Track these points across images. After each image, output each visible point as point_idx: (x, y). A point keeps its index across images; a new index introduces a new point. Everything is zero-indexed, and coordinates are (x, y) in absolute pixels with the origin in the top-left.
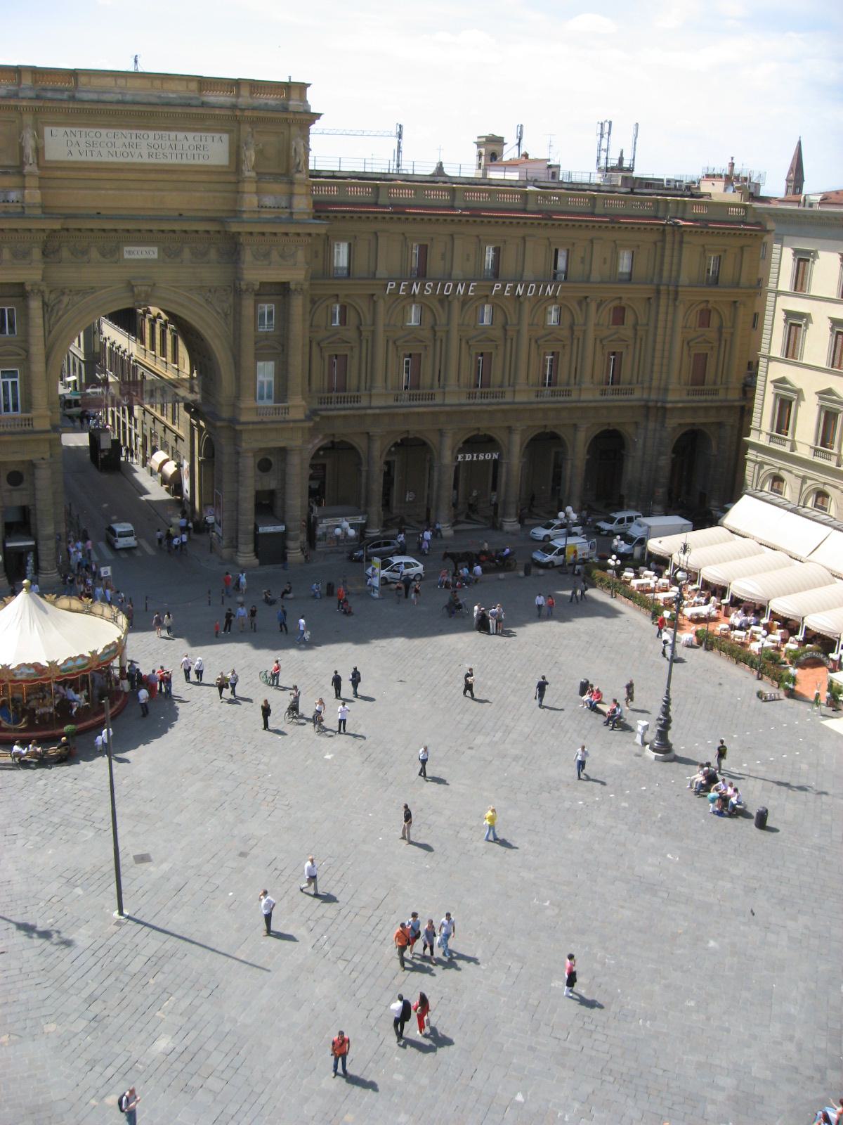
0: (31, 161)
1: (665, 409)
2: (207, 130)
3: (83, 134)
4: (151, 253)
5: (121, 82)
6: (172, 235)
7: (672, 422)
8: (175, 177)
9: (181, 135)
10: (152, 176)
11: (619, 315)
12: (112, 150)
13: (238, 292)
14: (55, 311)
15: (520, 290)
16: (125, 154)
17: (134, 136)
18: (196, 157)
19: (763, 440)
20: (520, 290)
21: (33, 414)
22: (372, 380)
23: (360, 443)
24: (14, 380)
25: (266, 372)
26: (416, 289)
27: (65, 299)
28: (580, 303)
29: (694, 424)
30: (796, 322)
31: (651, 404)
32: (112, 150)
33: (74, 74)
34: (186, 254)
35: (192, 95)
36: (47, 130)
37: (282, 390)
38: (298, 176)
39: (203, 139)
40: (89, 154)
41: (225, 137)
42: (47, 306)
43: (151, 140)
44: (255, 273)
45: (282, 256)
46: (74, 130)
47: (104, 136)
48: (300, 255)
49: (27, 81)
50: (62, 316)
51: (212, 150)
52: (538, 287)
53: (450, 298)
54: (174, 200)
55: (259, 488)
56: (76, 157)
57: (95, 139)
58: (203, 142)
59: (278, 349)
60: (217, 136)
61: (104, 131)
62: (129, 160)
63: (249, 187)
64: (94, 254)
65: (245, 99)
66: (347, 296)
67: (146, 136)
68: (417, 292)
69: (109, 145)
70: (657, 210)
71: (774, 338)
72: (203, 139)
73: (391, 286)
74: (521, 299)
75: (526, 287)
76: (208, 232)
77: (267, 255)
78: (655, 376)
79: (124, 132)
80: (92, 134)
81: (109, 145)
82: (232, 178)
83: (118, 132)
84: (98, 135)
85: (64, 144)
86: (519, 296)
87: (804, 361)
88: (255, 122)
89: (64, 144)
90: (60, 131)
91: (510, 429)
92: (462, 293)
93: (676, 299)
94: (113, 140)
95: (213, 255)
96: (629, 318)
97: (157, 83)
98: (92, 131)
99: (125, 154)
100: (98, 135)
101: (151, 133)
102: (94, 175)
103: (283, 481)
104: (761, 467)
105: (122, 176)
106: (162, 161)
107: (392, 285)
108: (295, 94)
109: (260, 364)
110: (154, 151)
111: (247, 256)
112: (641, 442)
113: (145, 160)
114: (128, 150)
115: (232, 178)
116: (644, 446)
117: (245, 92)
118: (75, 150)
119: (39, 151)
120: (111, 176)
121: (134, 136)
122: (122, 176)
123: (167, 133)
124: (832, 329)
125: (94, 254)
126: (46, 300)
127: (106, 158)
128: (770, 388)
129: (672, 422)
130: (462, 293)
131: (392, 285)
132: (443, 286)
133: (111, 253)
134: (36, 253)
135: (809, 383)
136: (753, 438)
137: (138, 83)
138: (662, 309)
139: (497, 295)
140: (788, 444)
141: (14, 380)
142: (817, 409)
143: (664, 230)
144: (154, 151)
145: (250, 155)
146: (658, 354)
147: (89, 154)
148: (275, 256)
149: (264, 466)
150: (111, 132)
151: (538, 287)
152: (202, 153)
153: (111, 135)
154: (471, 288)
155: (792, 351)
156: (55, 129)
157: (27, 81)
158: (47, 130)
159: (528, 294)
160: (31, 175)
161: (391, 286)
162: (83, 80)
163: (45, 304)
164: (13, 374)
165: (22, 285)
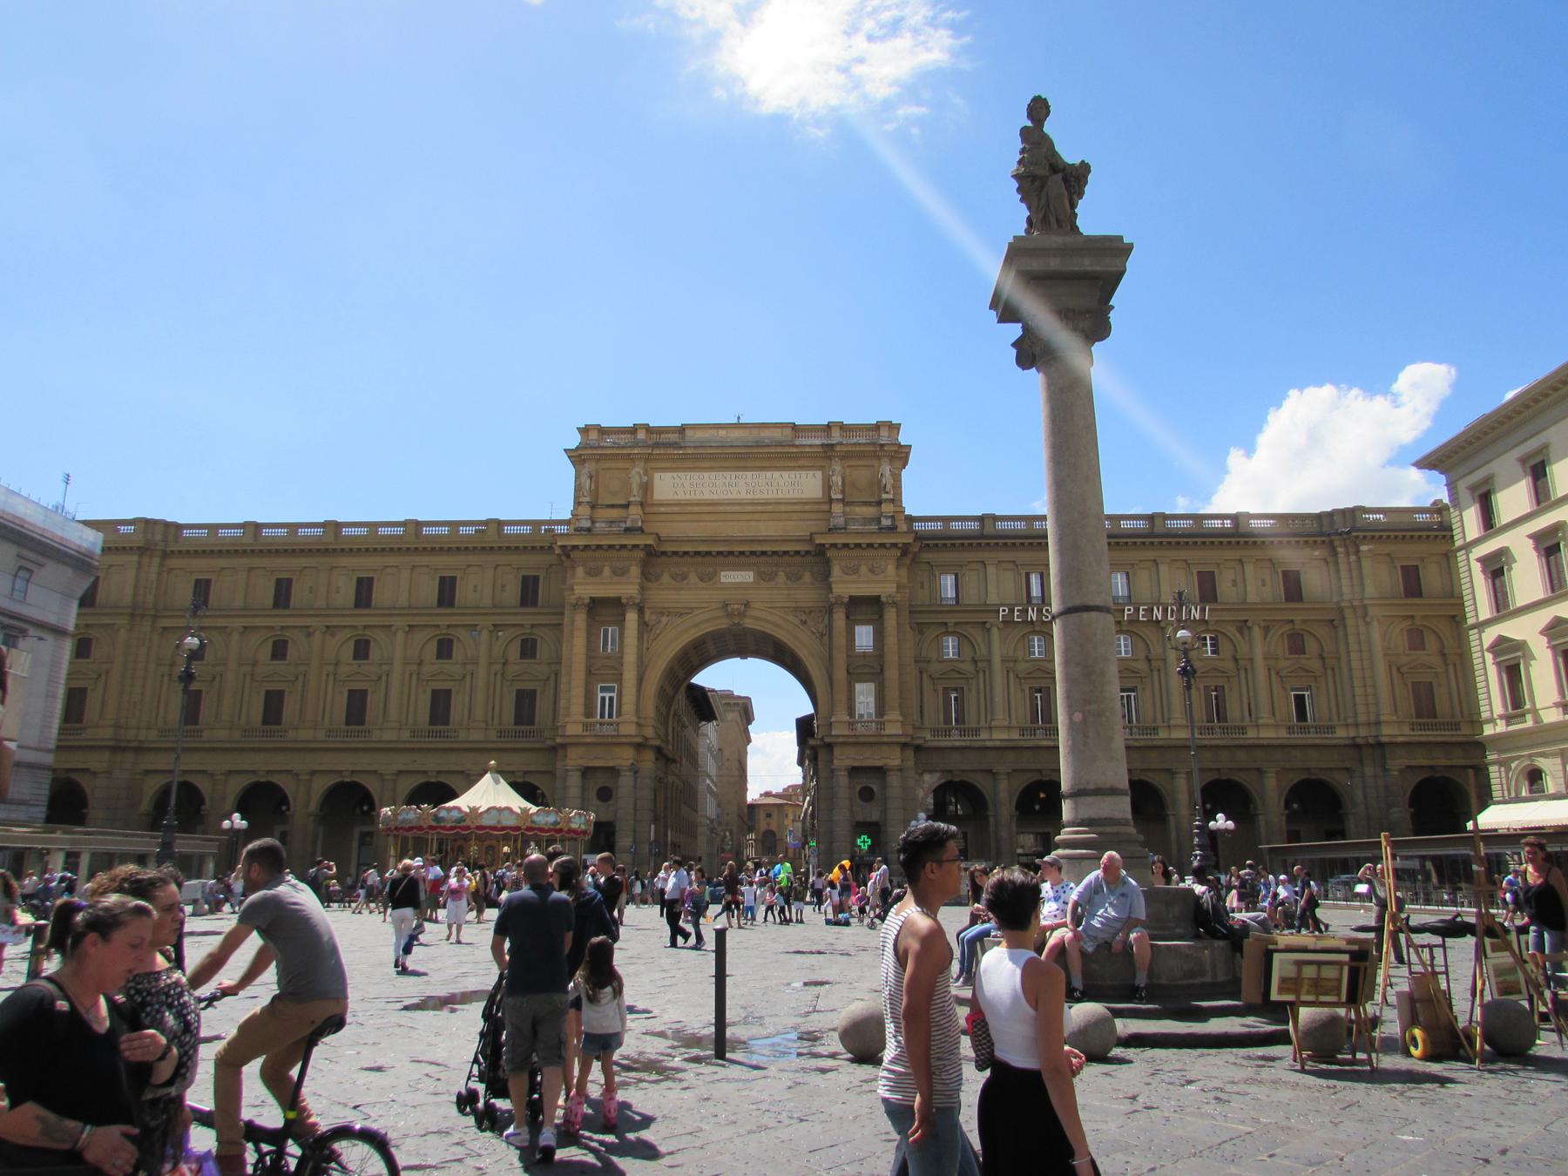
1: (1381, 745)
2: (801, 468)
4: (747, 576)
5: (722, 433)
6: (762, 557)
7: (1396, 763)
8: (770, 508)
9: (776, 474)
10: (749, 508)
11: (1296, 644)
13: (830, 611)
15: (1158, 614)
19: (1501, 727)
22: (993, 713)
23: (981, 782)
25: (865, 697)
27: (664, 620)
28: (1240, 631)
29: (1432, 767)
30: (1496, 568)
31: (1360, 741)
33: (682, 429)
36: (657, 476)
37: (881, 709)
38: (885, 496)
41: (819, 474)
44: (845, 586)
45: (872, 571)
47: (708, 477)
48: (891, 568)
49: (641, 435)
51: (805, 484)
54: (769, 529)
55: (860, 818)
56: (681, 496)
59: (871, 668)
61: (706, 475)
62: (729, 496)
64: (693, 578)
65: (836, 437)
70: (1321, 526)
71: (1480, 602)
76: (797, 553)
77: (856, 571)
78: (1361, 709)
82: (826, 507)
85: (670, 486)
86: (1158, 622)
87: (1519, 604)
88: (845, 457)
89: (670, 486)
90: (668, 475)
91: (1171, 772)
93: (1365, 615)
95: (807, 578)
96: (1311, 646)
97: (755, 431)
98: (695, 475)
102: (696, 509)
103: (885, 811)
104: (1508, 770)
105: (721, 509)
106: (758, 496)
108: (884, 433)
109: (859, 687)
111: (836, 571)
112: (1359, 793)
113: (744, 496)
115: (826, 507)
116: (1365, 798)
117: (836, 433)
119: (647, 488)
120: (710, 509)
122: (721, 509)
124: (1536, 549)
125: (693, 578)
127: (707, 496)
128: (1489, 657)
129: (1396, 763)
133: (708, 578)
134: (635, 571)
135: (1526, 629)
136: (1488, 730)
137: (736, 434)
138: (1350, 630)
139: (1131, 622)
140: (1529, 717)
142: (1549, 653)
143: (1331, 542)
145: (837, 479)
146: (1357, 683)
148: (864, 569)
149: (867, 794)
155: (1502, 606)
157: (641, 435)
158: (657, 476)
160: (635, 503)
162: (689, 433)
163: (644, 626)
164: (611, 689)
165: (619, 599)
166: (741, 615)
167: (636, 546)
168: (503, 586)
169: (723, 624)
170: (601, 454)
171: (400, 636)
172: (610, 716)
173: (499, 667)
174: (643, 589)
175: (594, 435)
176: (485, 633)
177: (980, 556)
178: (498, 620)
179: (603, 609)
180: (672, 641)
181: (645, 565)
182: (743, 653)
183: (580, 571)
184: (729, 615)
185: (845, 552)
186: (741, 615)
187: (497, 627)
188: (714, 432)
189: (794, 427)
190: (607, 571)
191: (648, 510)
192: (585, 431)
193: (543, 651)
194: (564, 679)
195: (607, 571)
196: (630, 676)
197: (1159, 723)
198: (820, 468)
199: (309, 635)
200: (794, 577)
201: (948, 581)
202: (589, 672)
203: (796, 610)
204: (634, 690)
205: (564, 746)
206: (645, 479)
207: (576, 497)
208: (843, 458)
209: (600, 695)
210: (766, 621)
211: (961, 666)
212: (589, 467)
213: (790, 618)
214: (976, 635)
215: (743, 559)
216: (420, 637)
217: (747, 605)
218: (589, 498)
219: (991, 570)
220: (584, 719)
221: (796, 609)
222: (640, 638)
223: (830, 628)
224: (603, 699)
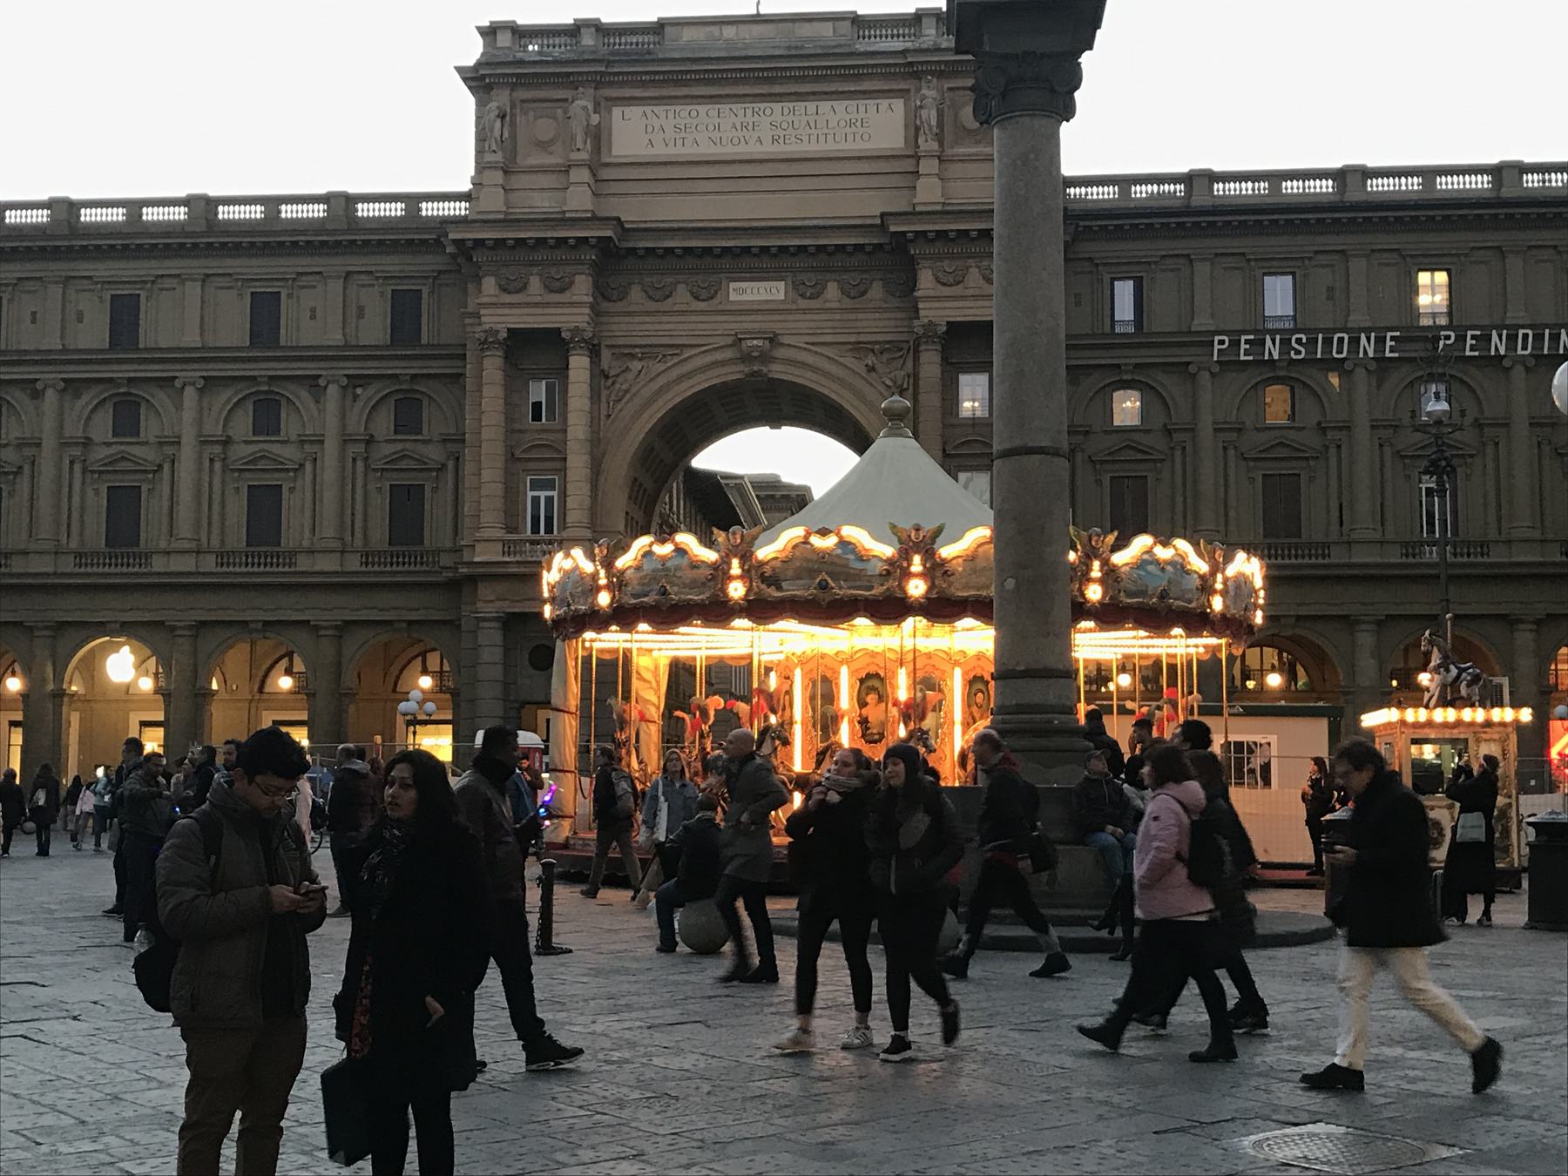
0: (579, 145)
3: (671, 115)
4: (773, 291)
5: (729, 32)
9: (825, 106)
12: (716, 135)
14: (617, 386)
15: (1498, 344)
16: (736, 141)
17: (749, 112)
18: (850, 138)
20: (1498, 344)
21: (565, 534)
24: (549, 493)
26: (1272, 350)
27: (636, 365)
32: (716, 135)
33: (660, 28)
34: (832, 290)
35: (843, 40)
36: (617, 112)
39: (862, 109)
40: (679, 142)
41: (898, 104)
42: (607, 377)
43: (777, 117)
44: (940, 305)
46: (655, 109)
49: (588, 40)
50: (627, 391)
52: (1539, 338)
53: (1348, 366)
57: (688, 120)
58: (862, 114)
60: (884, 103)
61: (702, 109)
62: (741, 150)
63: (928, 166)
64: (682, 296)
66: (1137, 366)
67: (768, 112)
68: (1276, 356)
69: (711, 127)
72: (862, 109)
73: (1220, 343)
74: (1507, 363)
75: (1512, 339)
76: (859, 248)
79: (733, 106)
80: (684, 114)
81: (711, 127)
82: (908, 165)
83: (725, 108)
84: (694, 113)
86: (1500, 358)
90: (634, 112)
92: (1371, 355)
94: (717, 121)
95: (876, 291)
98: (684, 110)
99: (736, 141)
100: (694, 113)
101: (777, 107)
107: (1222, 342)
110: (782, 133)
111: (926, 281)
113: (768, 149)
114: (740, 134)
115: (908, 165)
118: (657, 138)
119: (598, 137)
121: (749, 112)
123: (803, 104)
125: (682, 296)
126: (605, 364)
127: (707, 150)
130: (1371, 355)
131: (1222, 342)
132: (1328, 342)
137: (757, 30)
141: (549, 493)
144: (782, 133)
147: (679, 142)
150: (713, 109)
151: (1539, 338)
152: (861, 131)
153: (713, 113)
154: (1389, 343)
156: (627, 110)
157: (588, 40)
159: (1520, 352)
161: (1220, 343)
163: (599, 376)
164: (549, 485)
166: (765, 358)
167: (583, 241)
168: (361, 313)
169: (733, 373)
170: (519, 77)
171: (190, 394)
172: (549, 530)
173: (361, 448)
174: (596, 312)
175: (504, 40)
176: (333, 390)
177: (1182, 246)
178: (352, 368)
179: (533, 351)
180: (653, 397)
181: (600, 273)
182: (776, 421)
183: (489, 284)
184: (746, 358)
185: (939, 247)
186: (765, 358)
187: (355, 381)
188: (715, 30)
189: (856, 20)
190: (535, 284)
191: (606, 174)
192: (489, 33)
193: (434, 423)
194: (468, 468)
195: (535, 284)
196: (578, 463)
197: (1492, 534)
198: (902, 93)
199: (37, 395)
200: (856, 293)
201: (1124, 292)
202: (511, 458)
203: (858, 348)
204: (586, 489)
205: (473, 580)
206: (595, 119)
207: (480, 152)
208: (940, 75)
209: (530, 494)
210: (804, 365)
211: (1145, 440)
212: (501, 98)
213: (848, 361)
214: (1171, 386)
215: (766, 263)
216: (224, 398)
217: (773, 340)
218: (497, 149)
219: (1202, 269)
220: (501, 534)
221: (858, 348)
222: (595, 396)
223: (915, 376)
224: (536, 500)
